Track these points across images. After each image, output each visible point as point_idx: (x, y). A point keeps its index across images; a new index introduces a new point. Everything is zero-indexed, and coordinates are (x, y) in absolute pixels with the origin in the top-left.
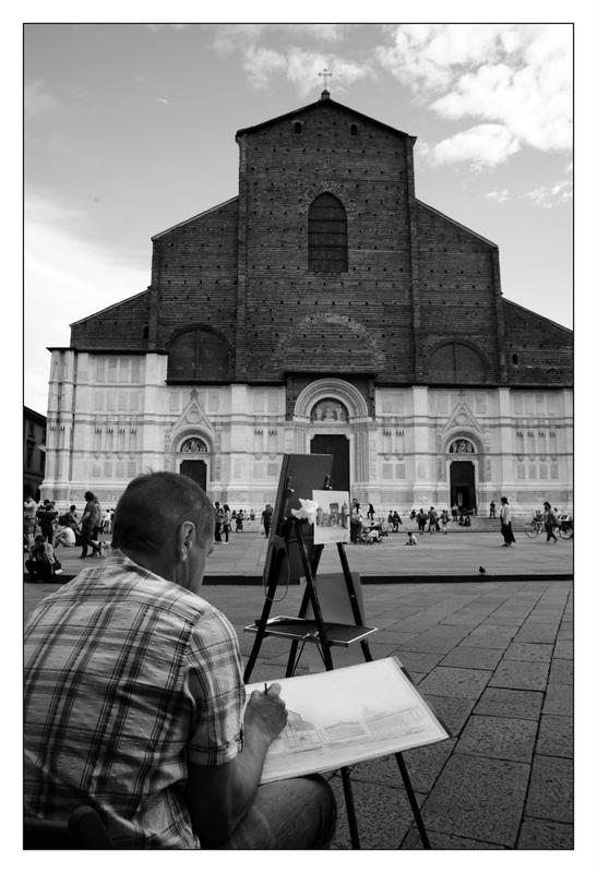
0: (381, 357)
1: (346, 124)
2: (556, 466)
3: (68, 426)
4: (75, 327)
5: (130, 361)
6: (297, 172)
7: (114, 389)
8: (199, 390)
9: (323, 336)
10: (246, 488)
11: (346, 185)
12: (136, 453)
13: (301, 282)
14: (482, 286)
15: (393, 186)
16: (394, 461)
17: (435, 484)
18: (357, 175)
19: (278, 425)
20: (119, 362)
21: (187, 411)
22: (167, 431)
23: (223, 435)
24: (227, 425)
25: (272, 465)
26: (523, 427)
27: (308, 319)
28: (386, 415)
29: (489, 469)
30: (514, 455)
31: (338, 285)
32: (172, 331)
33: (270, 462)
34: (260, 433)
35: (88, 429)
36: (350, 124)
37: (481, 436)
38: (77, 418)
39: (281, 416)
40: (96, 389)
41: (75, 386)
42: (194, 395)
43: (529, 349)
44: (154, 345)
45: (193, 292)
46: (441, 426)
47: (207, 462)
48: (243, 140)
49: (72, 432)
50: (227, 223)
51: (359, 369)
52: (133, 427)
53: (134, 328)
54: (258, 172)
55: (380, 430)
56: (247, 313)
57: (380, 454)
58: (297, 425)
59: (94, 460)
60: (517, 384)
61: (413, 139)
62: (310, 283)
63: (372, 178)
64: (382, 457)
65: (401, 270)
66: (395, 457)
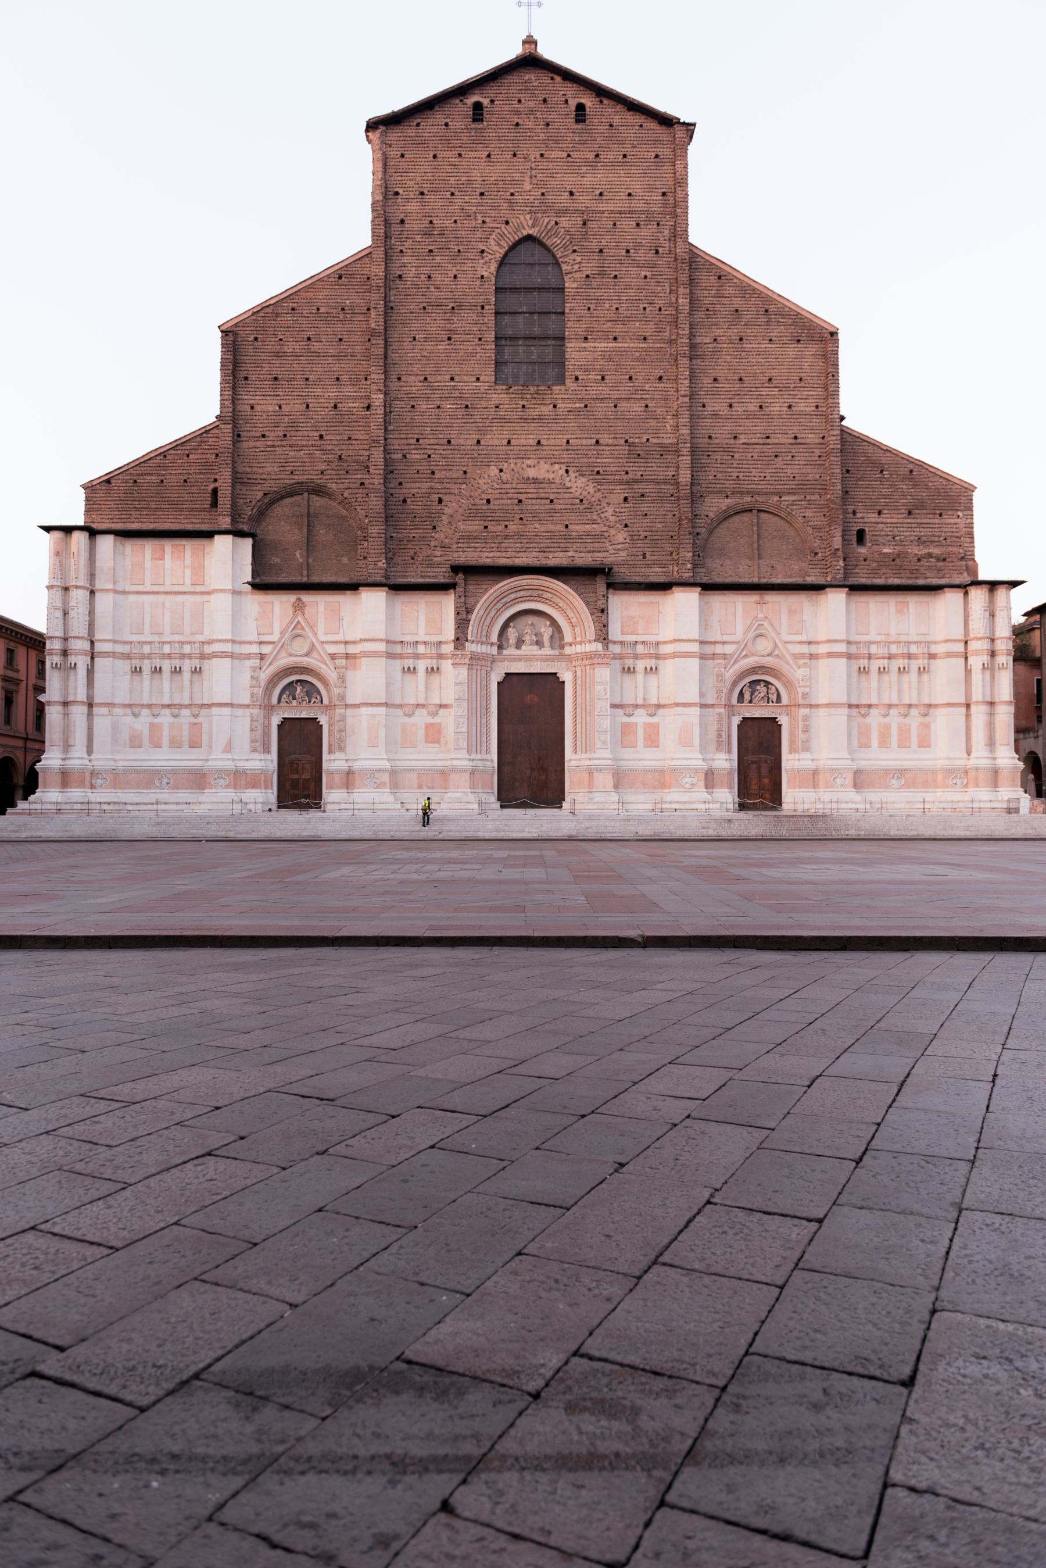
0: (621, 536)
1: (566, 101)
2: (927, 726)
3: (82, 662)
4: (90, 488)
6: (476, 199)
7: (161, 597)
8: (308, 598)
9: (520, 501)
10: (385, 764)
11: (564, 222)
12: (202, 706)
13: (484, 404)
15: (648, 221)
16: (640, 718)
17: (709, 756)
18: (584, 201)
19: (441, 656)
21: (287, 635)
22: (254, 669)
23: (350, 675)
25: (432, 724)
26: (870, 657)
27: (494, 471)
29: (806, 730)
30: (850, 706)
32: (260, 495)
33: (430, 720)
34: (411, 671)
35: (125, 666)
36: (573, 103)
37: (798, 673)
38: (99, 647)
39: (446, 643)
40: (132, 598)
41: (92, 592)
42: (299, 606)
43: (885, 518)
44: (228, 520)
45: (294, 424)
46: (724, 656)
47: (323, 720)
48: (375, 136)
49: (90, 672)
50: (353, 298)
51: (583, 559)
52: (196, 663)
53: (194, 489)
54: (408, 200)
55: (617, 664)
56: (387, 462)
57: (614, 706)
58: (474, 657)
59: (130, 719)
60: (863, 581)
61: (689, 128)
62: (497, 407)
63: (610, 207)
64: (620, 712)
65: (660, 378)
66: (640, 711)
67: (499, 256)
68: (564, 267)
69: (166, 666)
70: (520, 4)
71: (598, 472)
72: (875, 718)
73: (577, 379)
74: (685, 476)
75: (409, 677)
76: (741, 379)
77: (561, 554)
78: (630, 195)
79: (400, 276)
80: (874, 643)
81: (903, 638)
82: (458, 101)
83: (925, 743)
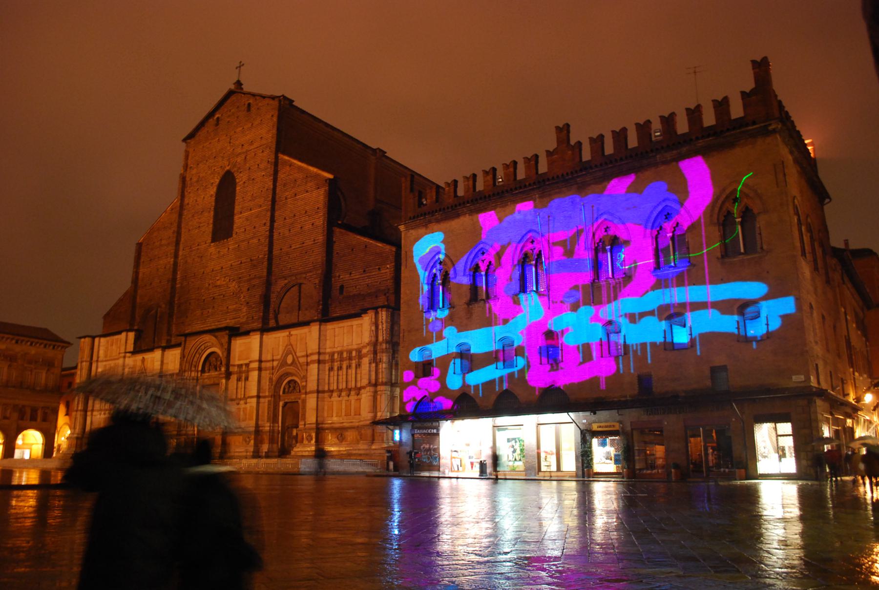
0: (244, 310)
1: (245, 104)
11: (239, 160)
18: (246, 147)
36: (247, 103)
63: (255, 146)
66: (242, 402)
67: (217, 183)
68: (237, 181)
70: (237, 68)
71: (240, 278)
76: (295, 216)
78: (261, 138)
79: (188, 204)
81: (350, 347)
82: (211, 120)
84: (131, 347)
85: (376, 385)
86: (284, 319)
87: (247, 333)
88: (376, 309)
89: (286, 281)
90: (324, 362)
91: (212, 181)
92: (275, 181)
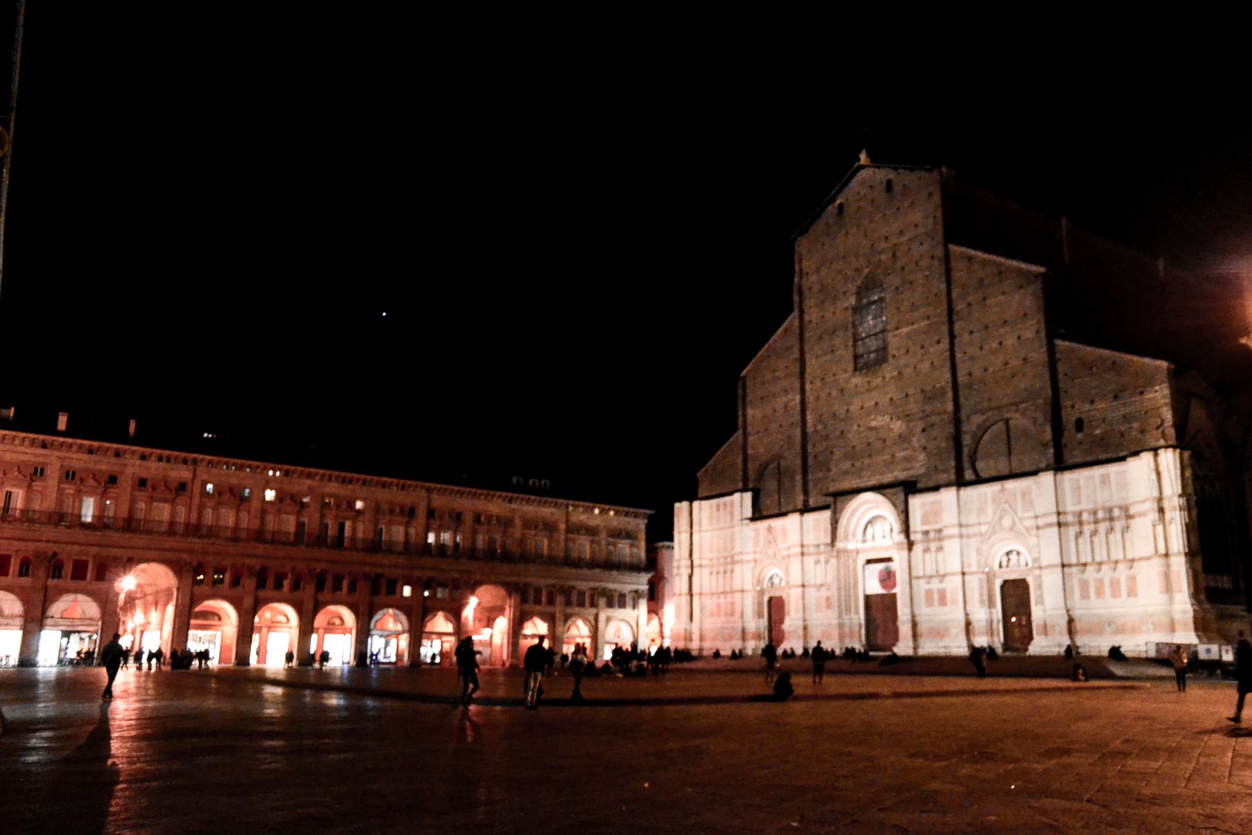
0: (922, 456)
2: (1132, 579)
5: (727, 499)
11: (883, 257)
14: (1029, 334)
16: (935, 585)
18: (893, 240)
20: (722, 506)
24: (789, 556)
28: (926, 528)
31: (879, 380)
34: (817, 562)
36: (885, 181)
40: (710, 534)
42: (770, 529)
46: (981, 534)
58: (838, 552)
60: (1078, 460)
66: (935, 580)
69: (722, 569)
72: (1091, 573)
73: (894, 356)
74: (950, 407)
75: (818, 566)
77: (890, 475)
79: (810, 322)
80: (1086, 510)
81: (1108, 505)
82: (830, 207)
83: (1132, 593)
84: (749, 514)
85: (1167, 555)
86: (983, 466)
87: (936, 488)
88: (1155, 450)
89: (984, 417)
90: (1066, 525)
91: (845, 289)
92: (949, 282)
